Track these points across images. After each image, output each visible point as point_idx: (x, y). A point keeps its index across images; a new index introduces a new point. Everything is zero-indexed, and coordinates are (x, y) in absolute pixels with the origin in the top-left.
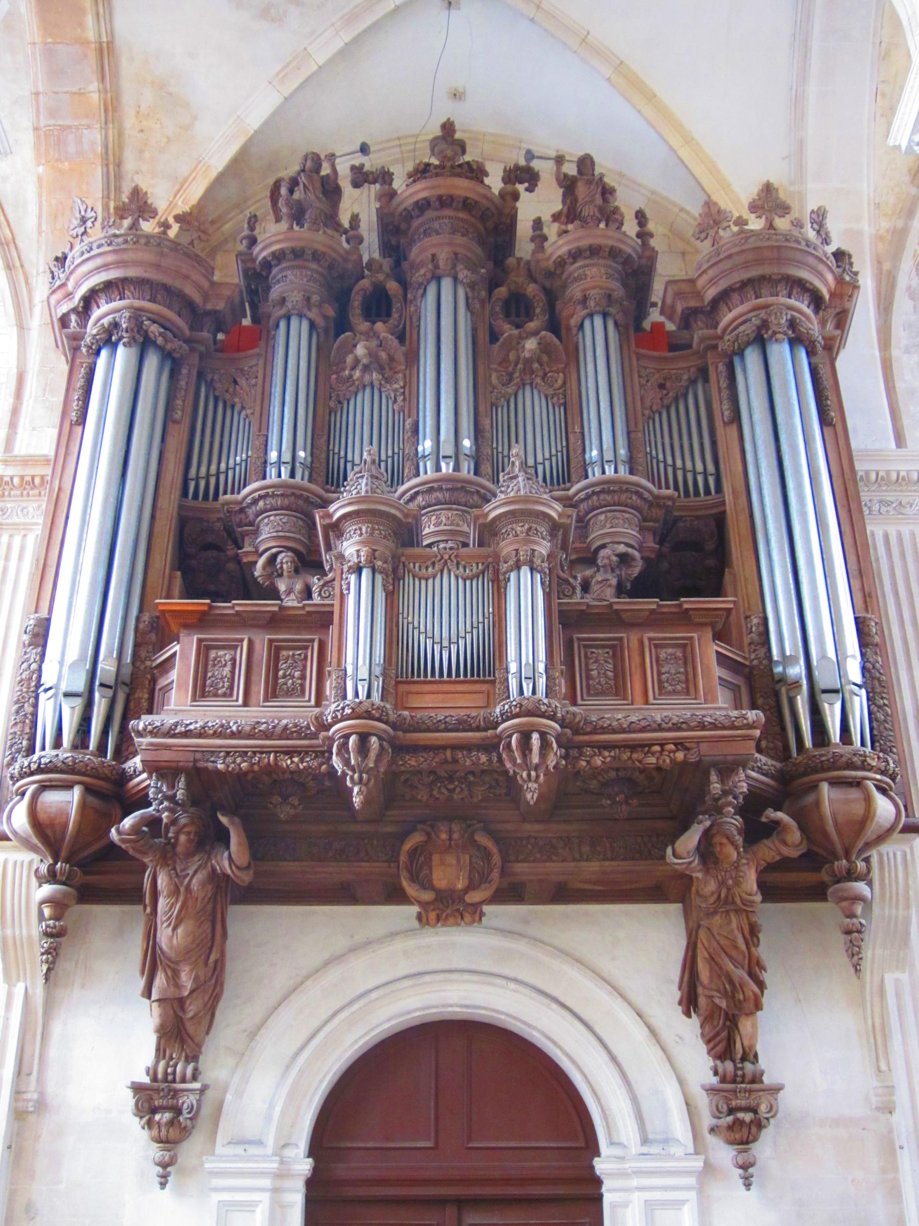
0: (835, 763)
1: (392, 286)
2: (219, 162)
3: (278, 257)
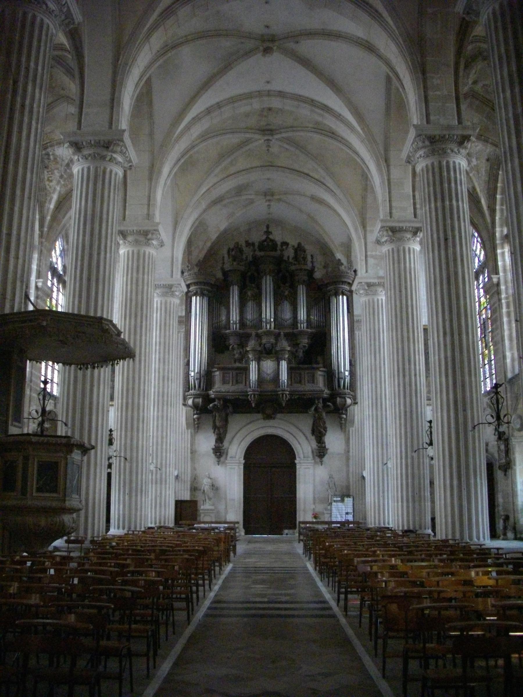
0: (340, 394)
1: (256, 274)
2: (214, 236)
3: (230, 271)
